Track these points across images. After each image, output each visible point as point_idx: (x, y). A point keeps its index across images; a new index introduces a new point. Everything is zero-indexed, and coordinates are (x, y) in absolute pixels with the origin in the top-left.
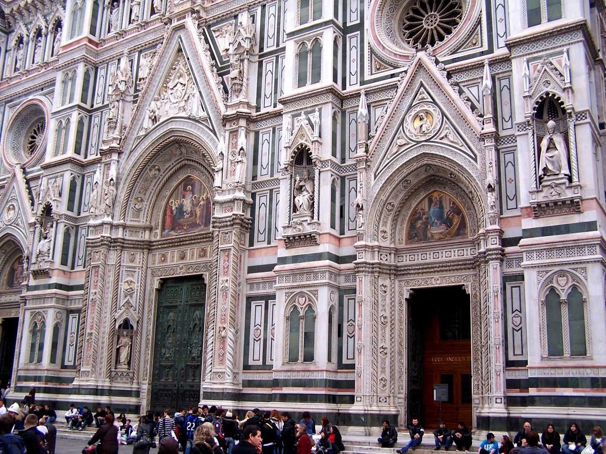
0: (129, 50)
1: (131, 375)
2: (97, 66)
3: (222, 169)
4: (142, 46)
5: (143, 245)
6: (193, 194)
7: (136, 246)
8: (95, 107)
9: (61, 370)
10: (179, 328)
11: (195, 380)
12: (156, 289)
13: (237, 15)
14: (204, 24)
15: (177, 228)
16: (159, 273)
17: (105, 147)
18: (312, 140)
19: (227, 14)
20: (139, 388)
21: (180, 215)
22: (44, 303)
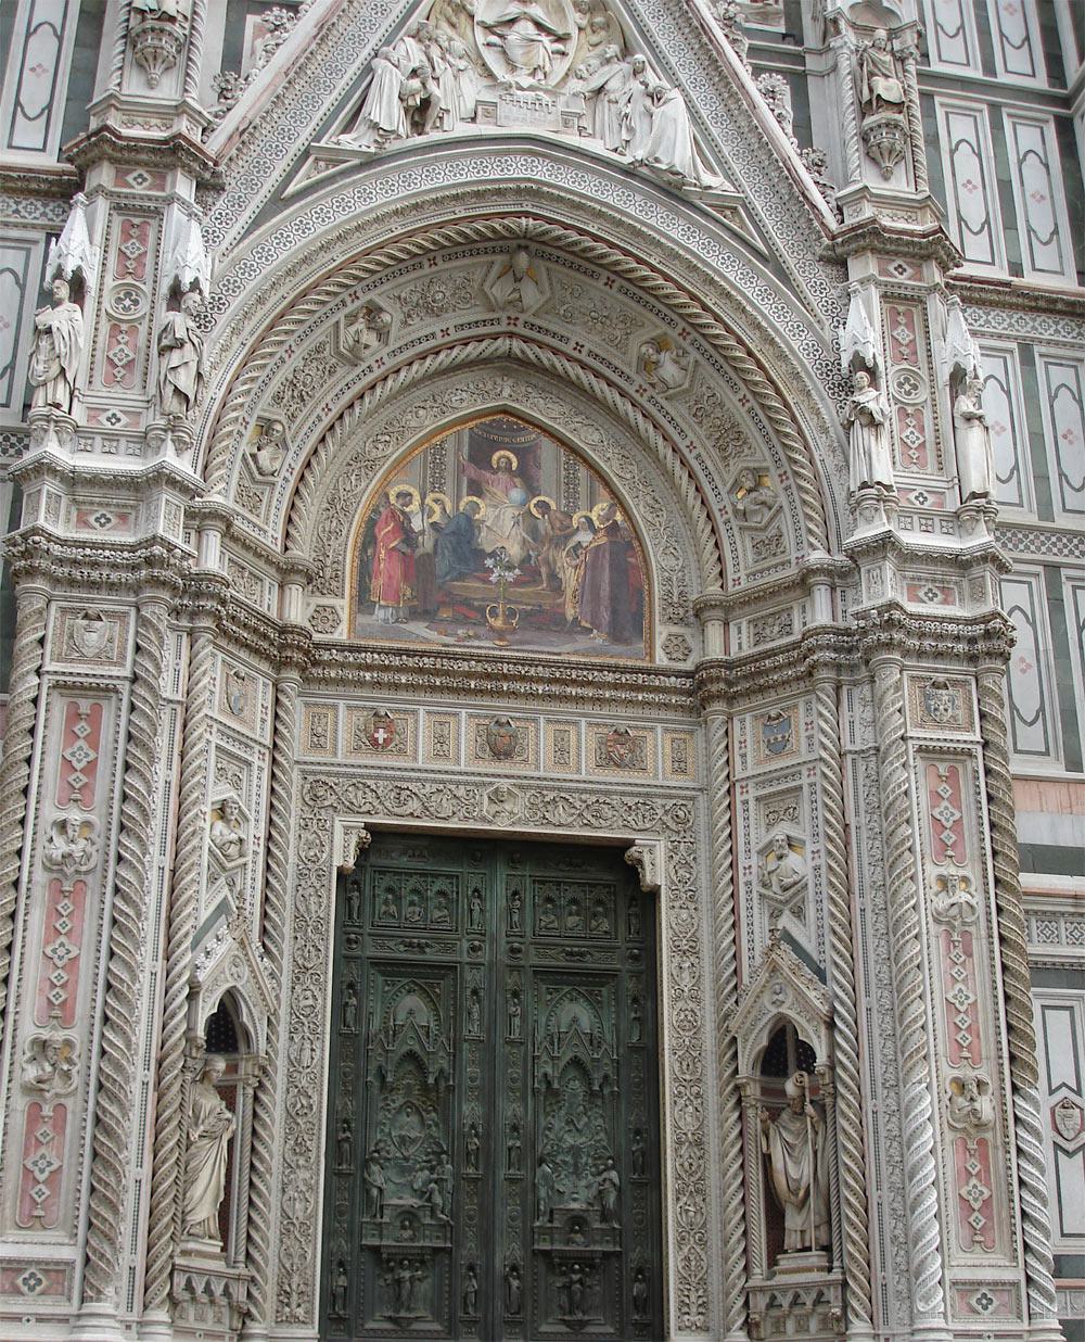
1: (239, 1293)
5: (282, 647)
6: (532, 490)
12: (341, 872)
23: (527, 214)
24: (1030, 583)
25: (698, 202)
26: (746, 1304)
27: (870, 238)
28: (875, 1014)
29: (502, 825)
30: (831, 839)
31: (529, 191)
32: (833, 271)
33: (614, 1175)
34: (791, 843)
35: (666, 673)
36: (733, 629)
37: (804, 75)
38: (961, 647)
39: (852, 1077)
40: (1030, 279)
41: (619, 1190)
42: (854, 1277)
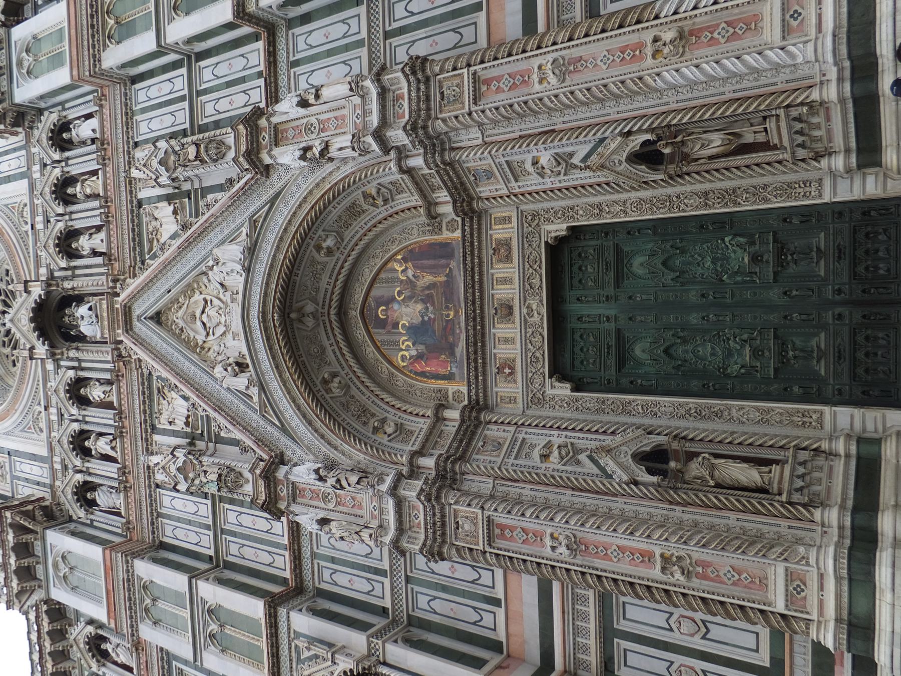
1: (803, 456)
3: (327, 142)
4: (146, 421)
6: (393, 299)
8: (213, 554)
11: (818, 249)
12: (573, 390)
20: (848, 437)
23: (273, 317)
24: (395, 47)
26: (803, 160)
27: (252, 155)
28: (620, 109)
29: (544, 311)
30: (528, 145)
31: (263, 317)
32: (272, 171)
33: (727, 239)
34: (535, 163)
35: (464, 231)
36: (438, 200)
37: (202, 188)
38: (422, 87)
39: (658, 118)
40: (262, 68)
41: (735, 235)
42: (782, 102)
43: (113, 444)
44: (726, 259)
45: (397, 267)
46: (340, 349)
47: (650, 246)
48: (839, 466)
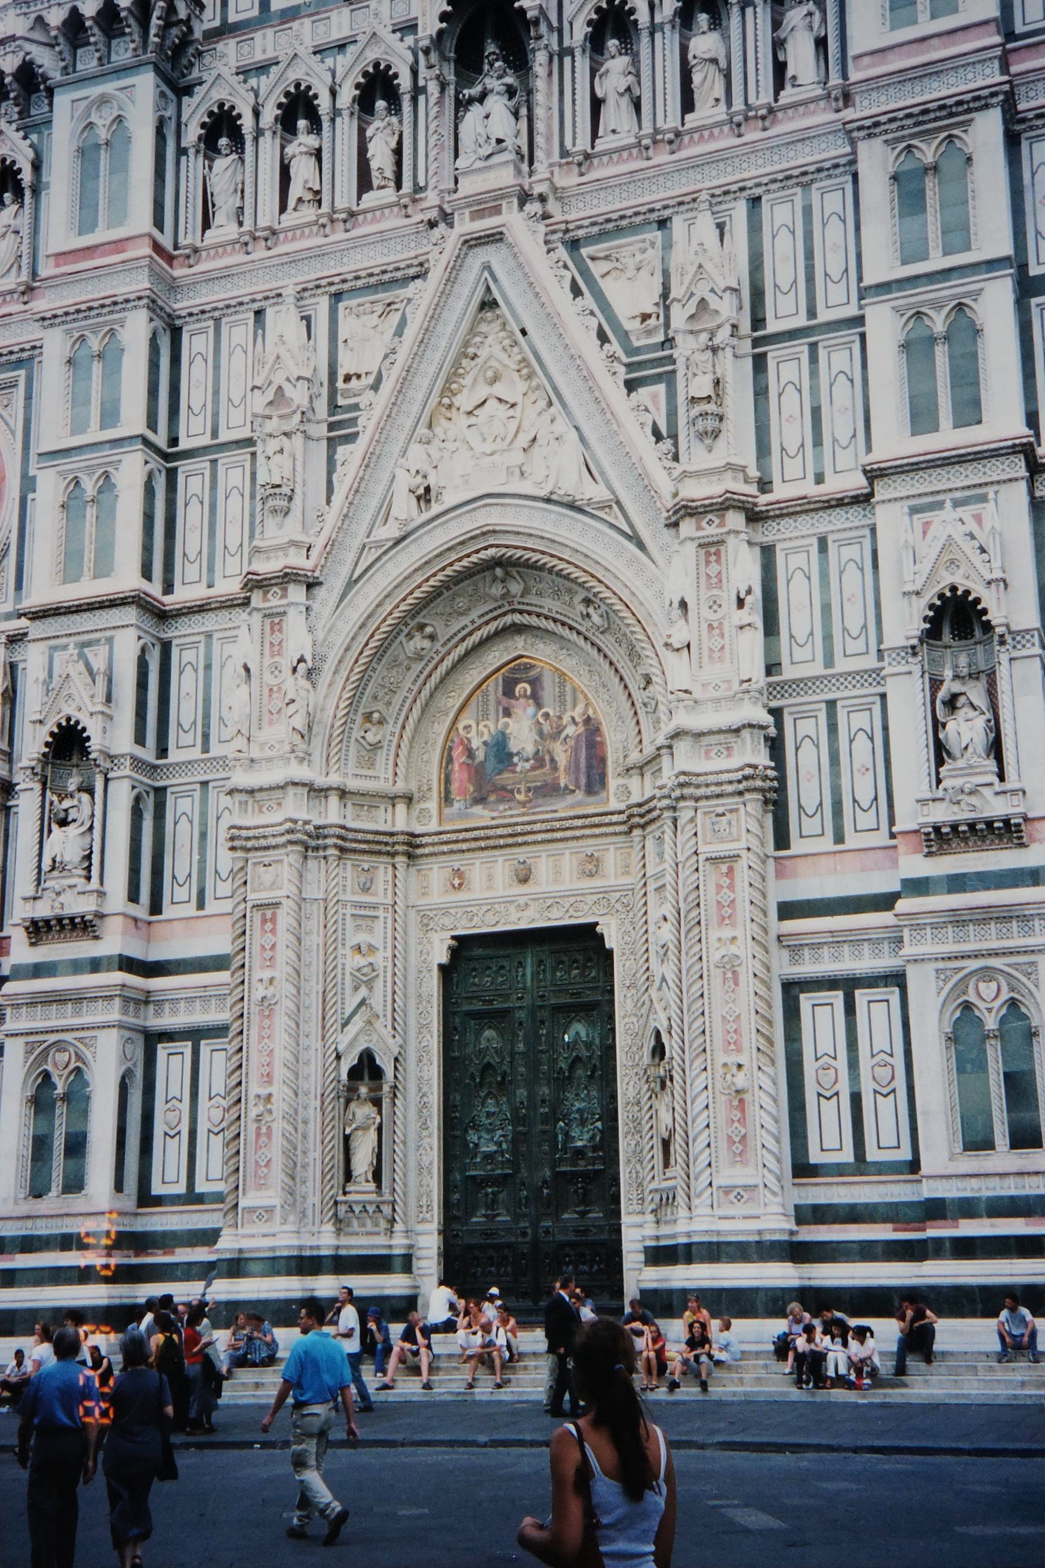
0: (299, 288)
2: (178, 322)
3: (688, 646)
4: (344, 281)
6: (539, 705)
7: (377, 847)
9: (140, 1210)
10: (522, 1069)
12: (442, 967)
13: (669, 219)
14: (560, 235)
15: (492, 798)
16: (447, 921)
17: (266, 567)
18: (988, 577)
19: (636, 214)
20: (411, 1247)
21: (501, 762)
22: (77, 1014)
23: (491, 546)
25: (587, 509)
29: (523, 925)
31: (489, 532)
32: (673, 531)
33: (599, 1124)
38: (730, 788)
43: (309, 196)
44: (583, 1122)
45: (580, 708)
46: (471, 634)
47: (597, 1041)
48: (381, 1240)
